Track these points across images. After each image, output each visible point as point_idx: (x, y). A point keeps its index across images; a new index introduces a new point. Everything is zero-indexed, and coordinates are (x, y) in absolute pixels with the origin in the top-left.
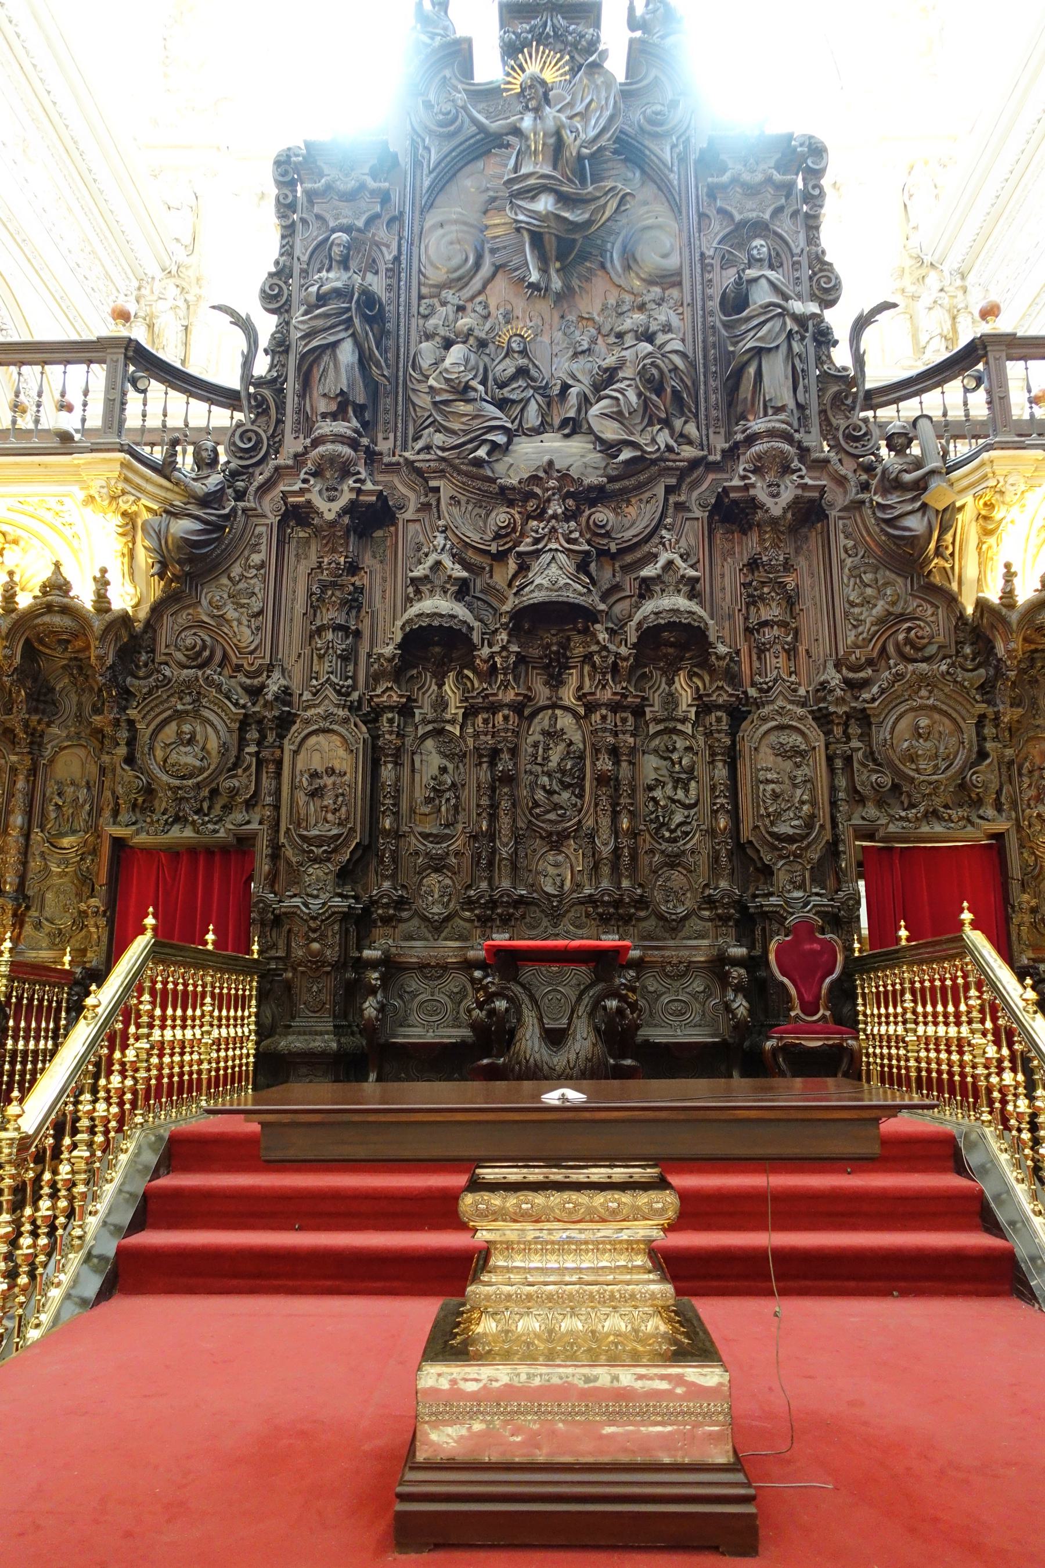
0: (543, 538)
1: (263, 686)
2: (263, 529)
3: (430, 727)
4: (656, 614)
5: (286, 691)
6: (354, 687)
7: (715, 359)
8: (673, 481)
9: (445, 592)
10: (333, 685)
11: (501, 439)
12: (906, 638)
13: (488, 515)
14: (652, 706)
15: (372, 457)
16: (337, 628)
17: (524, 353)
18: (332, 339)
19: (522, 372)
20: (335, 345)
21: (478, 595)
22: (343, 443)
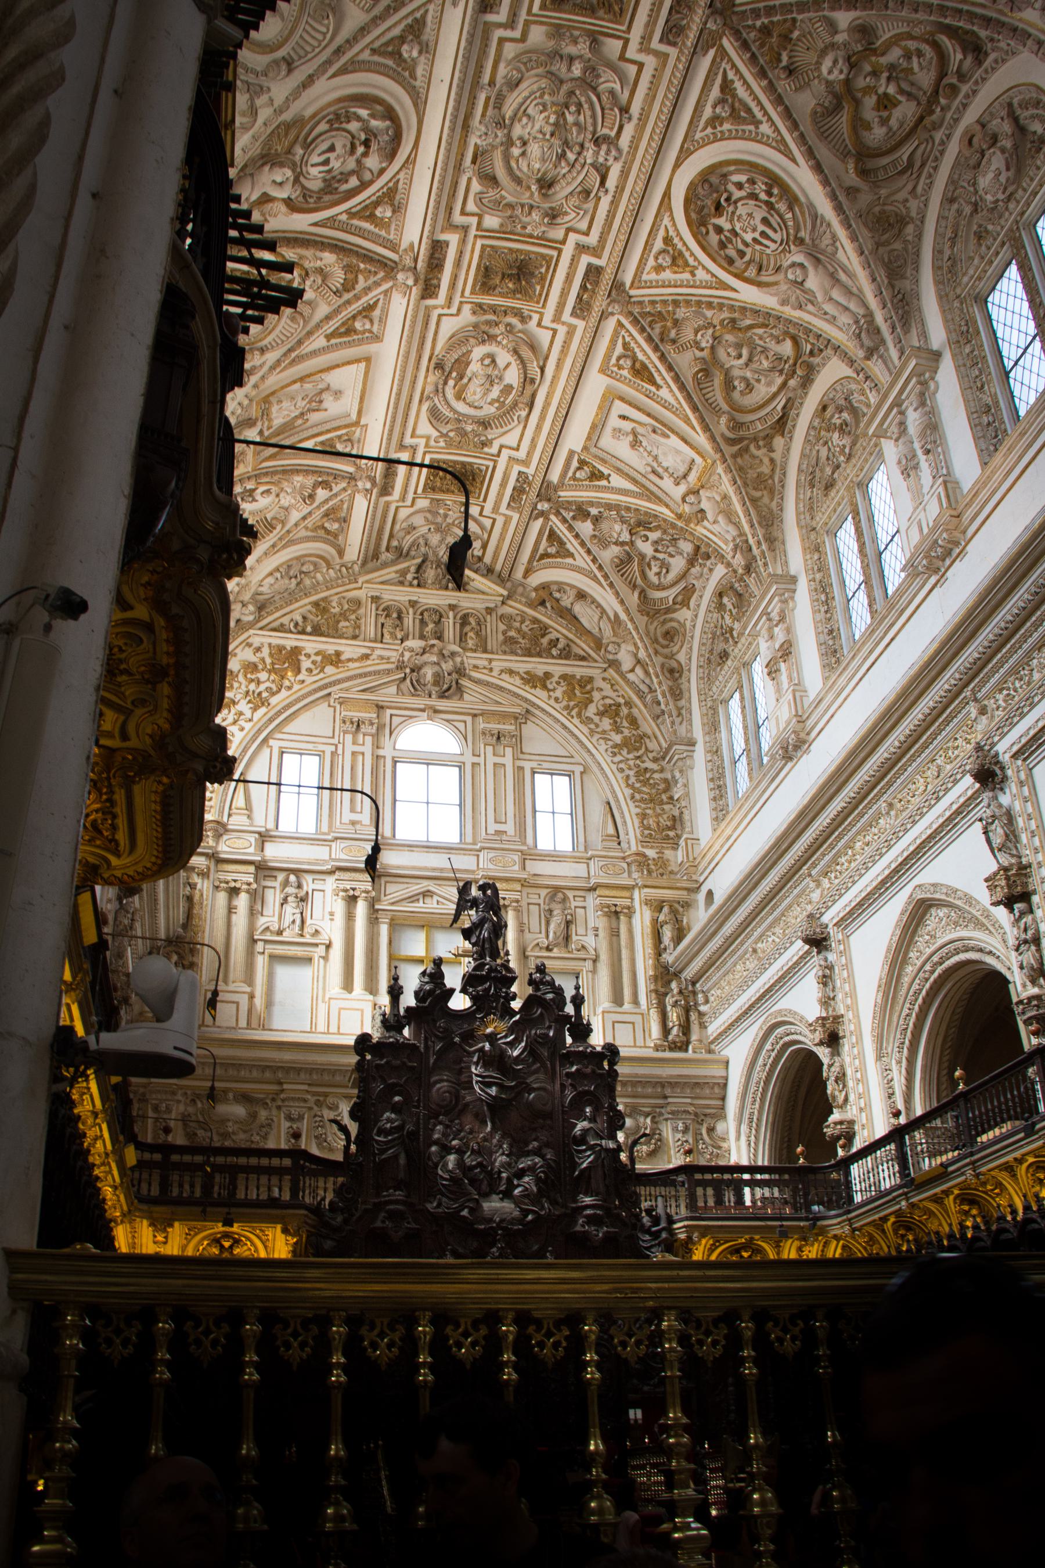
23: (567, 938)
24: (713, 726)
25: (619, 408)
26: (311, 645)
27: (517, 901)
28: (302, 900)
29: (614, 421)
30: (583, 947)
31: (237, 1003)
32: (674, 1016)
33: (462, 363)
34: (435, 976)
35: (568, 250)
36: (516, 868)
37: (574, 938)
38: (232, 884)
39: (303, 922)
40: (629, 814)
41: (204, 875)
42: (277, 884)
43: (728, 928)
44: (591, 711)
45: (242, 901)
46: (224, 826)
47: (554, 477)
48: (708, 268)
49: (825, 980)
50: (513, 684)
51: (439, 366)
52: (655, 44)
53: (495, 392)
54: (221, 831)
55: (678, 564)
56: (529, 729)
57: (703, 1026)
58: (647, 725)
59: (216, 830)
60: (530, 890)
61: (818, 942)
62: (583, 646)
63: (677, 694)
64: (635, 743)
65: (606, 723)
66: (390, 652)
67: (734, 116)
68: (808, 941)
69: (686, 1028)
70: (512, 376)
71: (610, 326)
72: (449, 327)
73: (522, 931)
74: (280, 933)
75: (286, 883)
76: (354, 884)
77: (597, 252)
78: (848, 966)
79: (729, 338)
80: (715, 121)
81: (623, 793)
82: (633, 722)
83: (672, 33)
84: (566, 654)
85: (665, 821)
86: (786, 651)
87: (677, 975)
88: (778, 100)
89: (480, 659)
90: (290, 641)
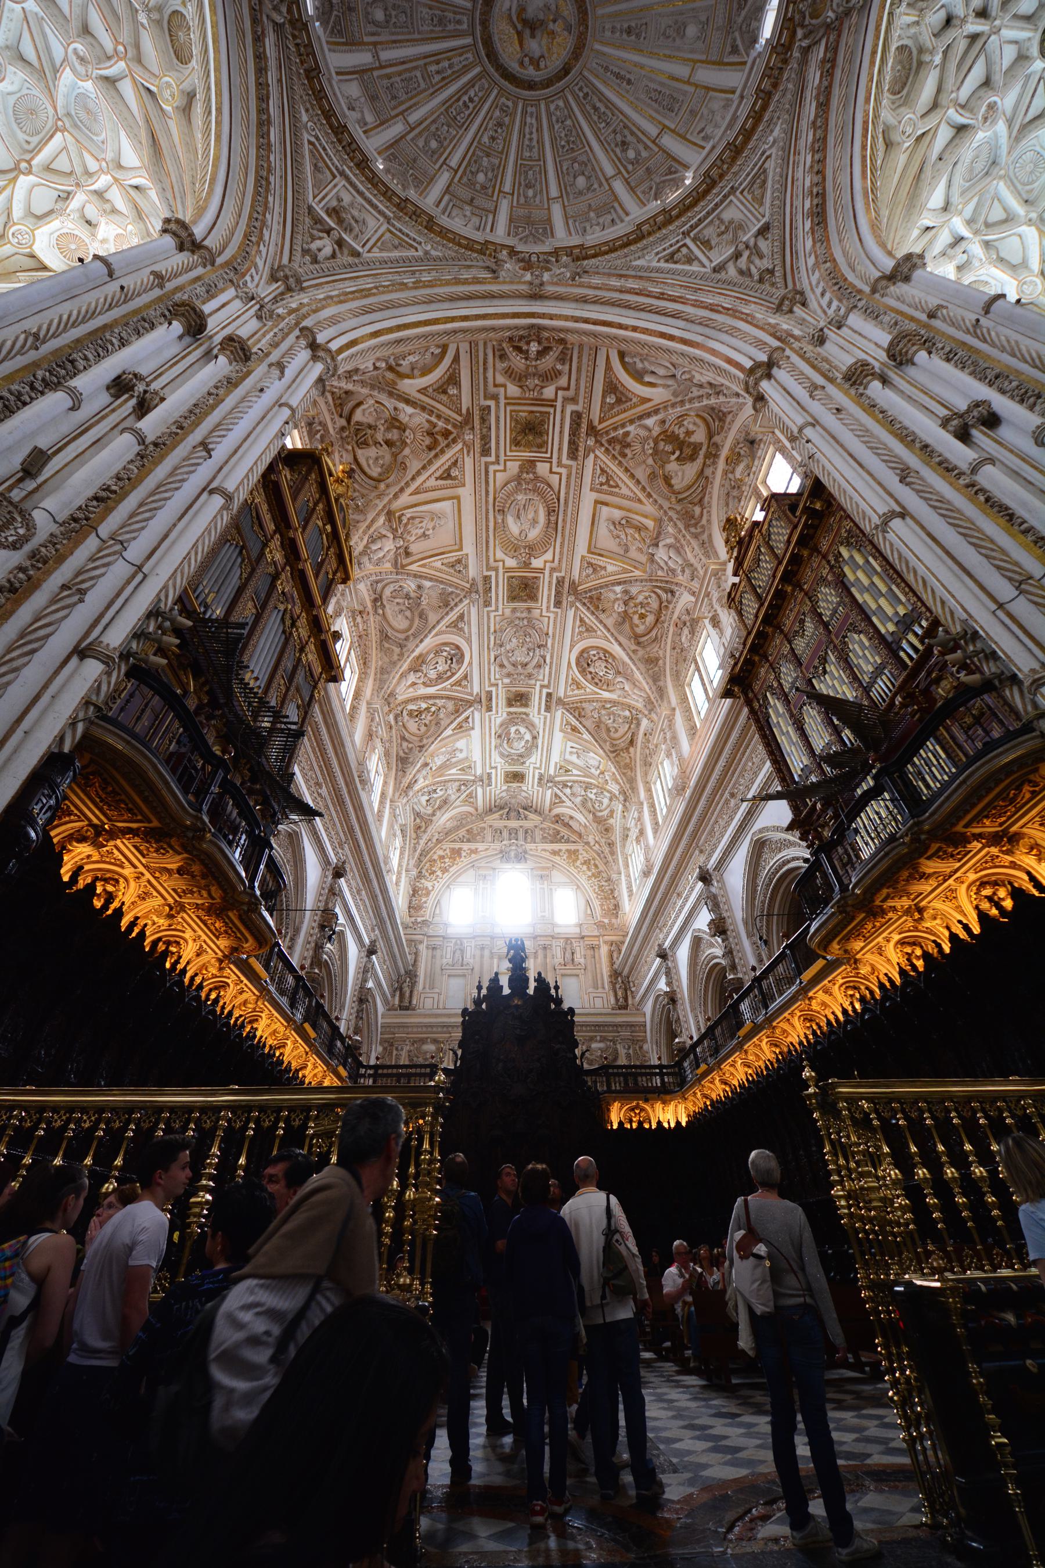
24: (627, 866)
25: (570, 744)
26: (466, 846)
29: (569, 749)
32: (620, 993)
33: (508, 734)
34: (495, 981)
35: (538, 688)
40: (596, 903)
41: (421, 942)
43: (634, 952)
44: (578, 863)
45: (438, 953)
47: (552, 772)
48: (590, 688)
49: (668, 974)
50: (547, 855)
51: (500, 736)
52: (552, 609)
53: (523, 743)
55: (606, 801)
56: (555, 873)
57: (633, 998)
58: (601, 867)
61: (663, 956)
62: (574, 837)
63: (613, 853)
64: (597, 875)
65: (585, 868)
66: (497, 846)
67: (587, 630)
68: (659, 956)
69: (626, 999)
70: (528, 737)
71: (559, 714)
72: (499, 721)
77: (548, 687)
78: (676, 967)
79: (603, 712)
80: (580, 633)
81: (593, 896)
82: (596, 866)
83: (558, 604)
84: (568, 841)
85: (612, 907)
86: (642, 832)
87: (620, 974)
88: (601, 622)
89: (532, 846)
90: (457, 846)
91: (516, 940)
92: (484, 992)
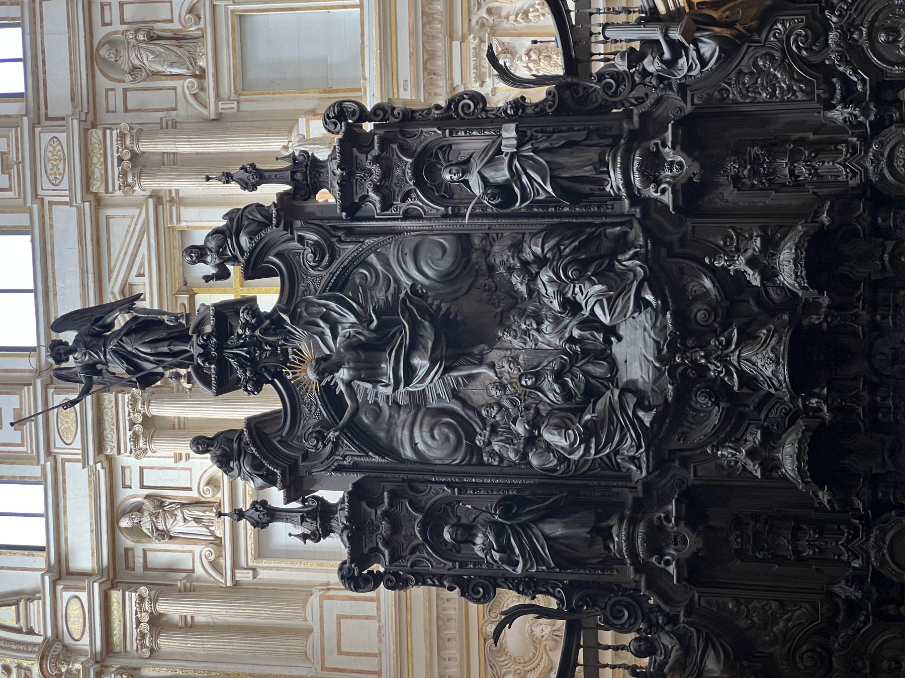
0: (725, 366)
1: (848, 601)
2: (702, 600)
3: (888, 461)
4: (797, 277)
5: (851, 581)
6: (848, 524)
7: (542, 207)
8: (663, 251)
9: (774, 448)
10: (848, 541)
11: (631, 400)
12: (805, 49)
13: (694, 410)
14: (870, 274)
15: (640, 507)
16: (795, 538)
17: (538, 375)
18: (542, 539)
19: (558, 376)
20: (546, 537)
21: (763, 417)
22: (634, 531)
23: (178, 38)
27: (122, 136)
28: (161, 505)
30: (190, 11)
31: (339, 617)
36: (62, 136)
37: (176, 26)
38: (145, 626)
39: (197, 503)
42: (139, 548)
45: (172, 609)
46: (48, 644)
54: (58, 647)
59: (57, 660)
60: (102, 106)
73: (175, 124)
74: (218, 542)
75: (136, 531)
76: (124, 423)
91: (59, 351)
92: (276, 497)
